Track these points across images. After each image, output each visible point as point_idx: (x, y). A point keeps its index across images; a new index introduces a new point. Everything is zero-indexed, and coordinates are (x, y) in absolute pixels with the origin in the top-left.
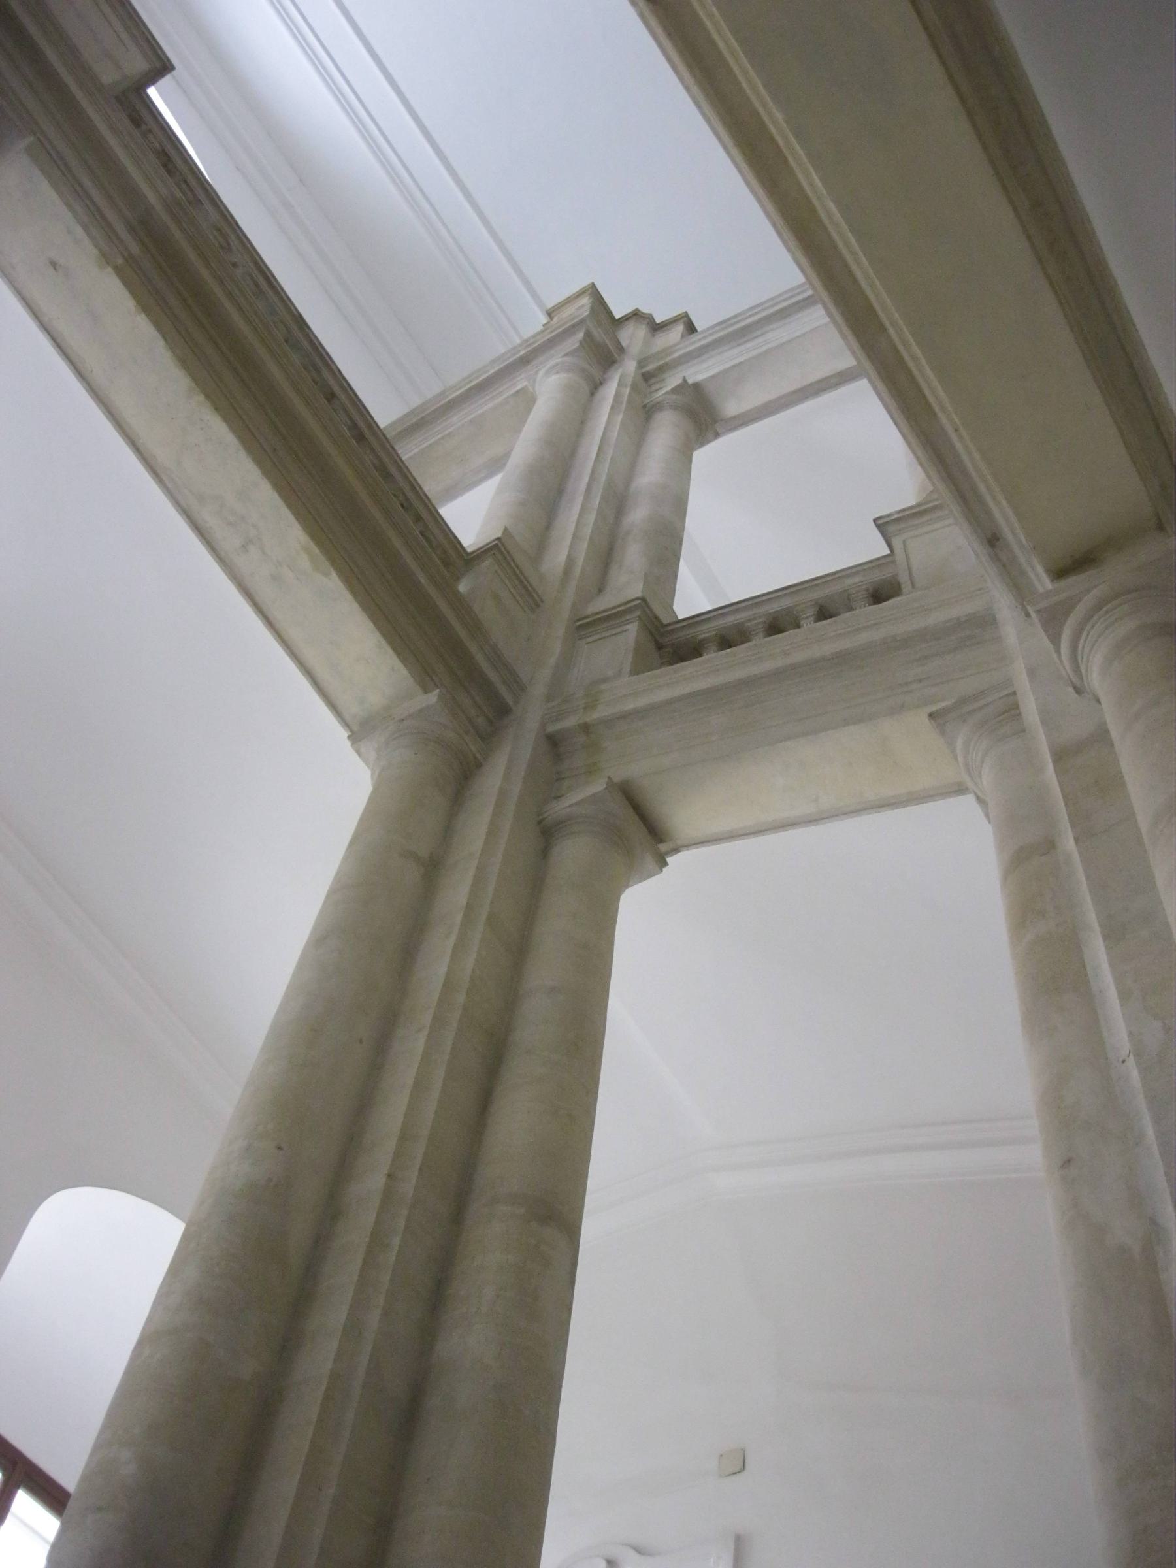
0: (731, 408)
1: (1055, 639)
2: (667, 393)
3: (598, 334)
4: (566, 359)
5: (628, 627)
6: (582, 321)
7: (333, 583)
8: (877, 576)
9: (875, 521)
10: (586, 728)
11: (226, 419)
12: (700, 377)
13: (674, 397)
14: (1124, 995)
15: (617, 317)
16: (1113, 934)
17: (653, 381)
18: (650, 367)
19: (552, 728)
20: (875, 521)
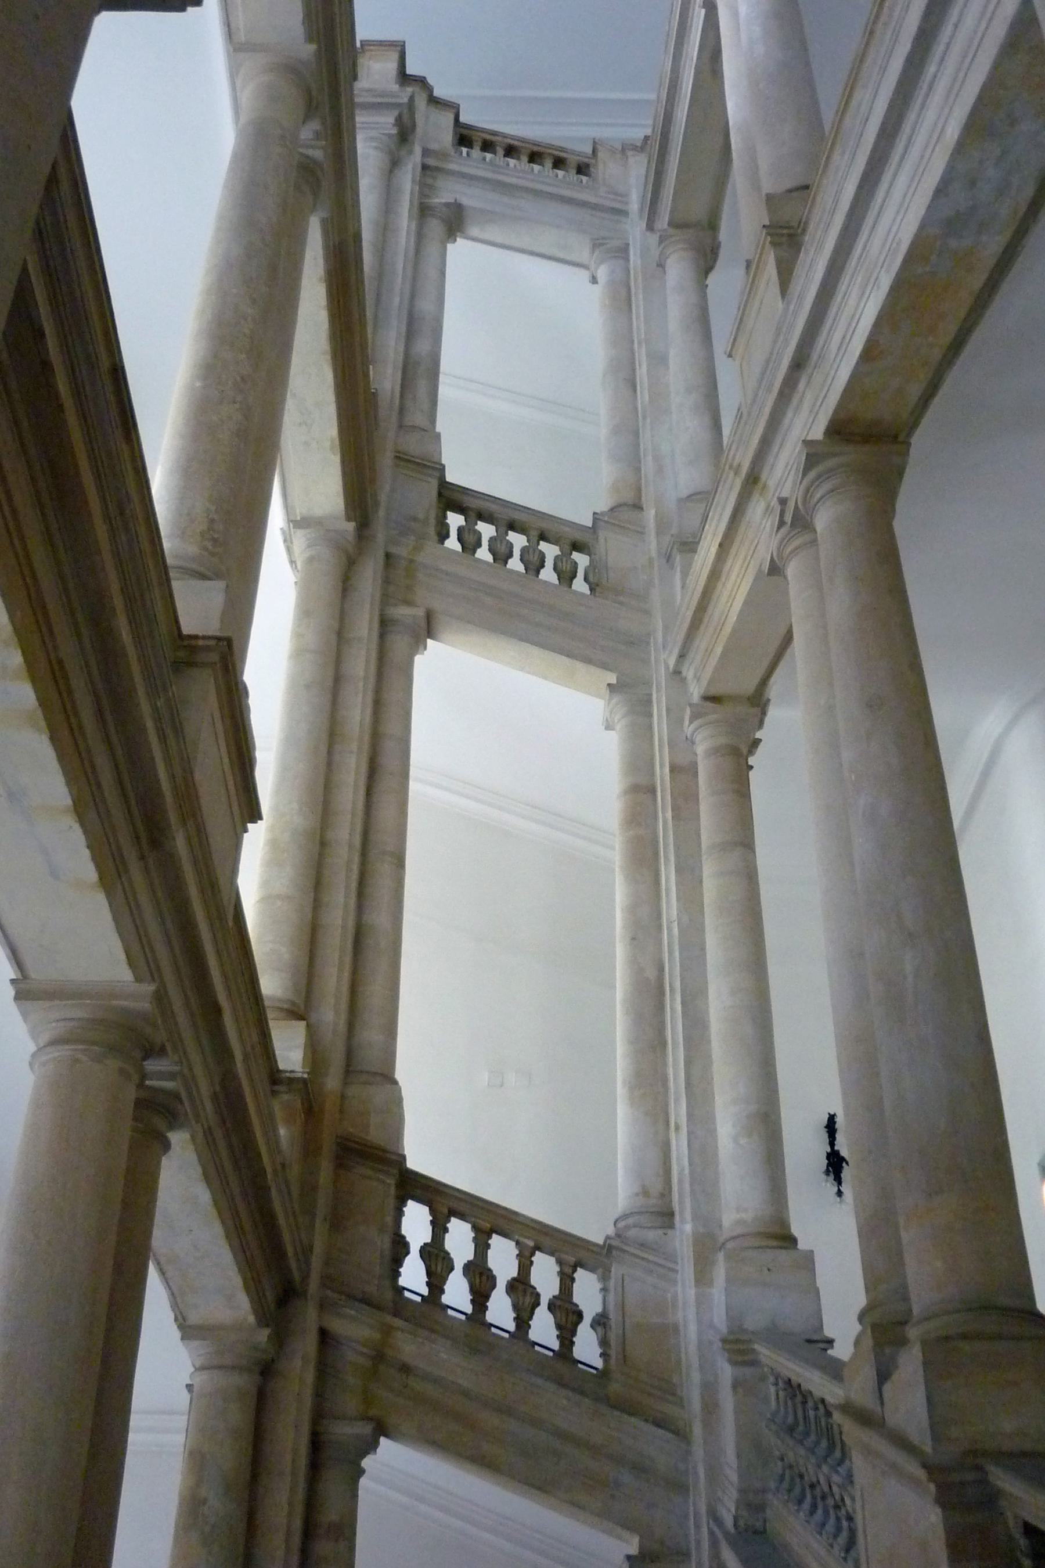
0: (474, 231)
1: (691, 722)
2: (440, 203)
3: (406, 118)
4: (384, 137)
5: (430, 479)
6: (399, 105)
7: (336, 459)
8: (578, 536)
9: (594, 513)
10: (411, 561)
11: (335, 371)
12: (465, 201)
13: (444, 209)
14: (678, 899)
15: (408, 72)
16: (679, 870)
17: (428, 173)
18: (431, 162)
19: (393, 550)
20: (594, 513)
